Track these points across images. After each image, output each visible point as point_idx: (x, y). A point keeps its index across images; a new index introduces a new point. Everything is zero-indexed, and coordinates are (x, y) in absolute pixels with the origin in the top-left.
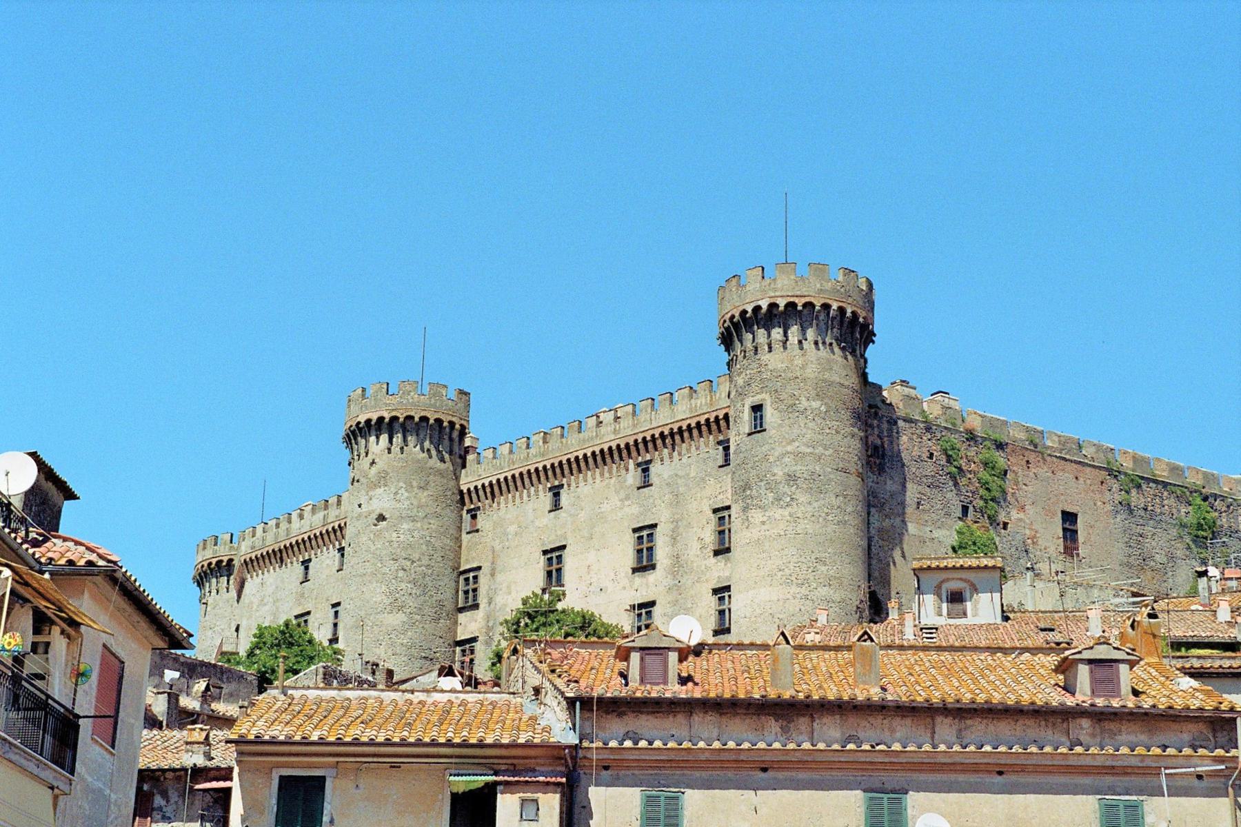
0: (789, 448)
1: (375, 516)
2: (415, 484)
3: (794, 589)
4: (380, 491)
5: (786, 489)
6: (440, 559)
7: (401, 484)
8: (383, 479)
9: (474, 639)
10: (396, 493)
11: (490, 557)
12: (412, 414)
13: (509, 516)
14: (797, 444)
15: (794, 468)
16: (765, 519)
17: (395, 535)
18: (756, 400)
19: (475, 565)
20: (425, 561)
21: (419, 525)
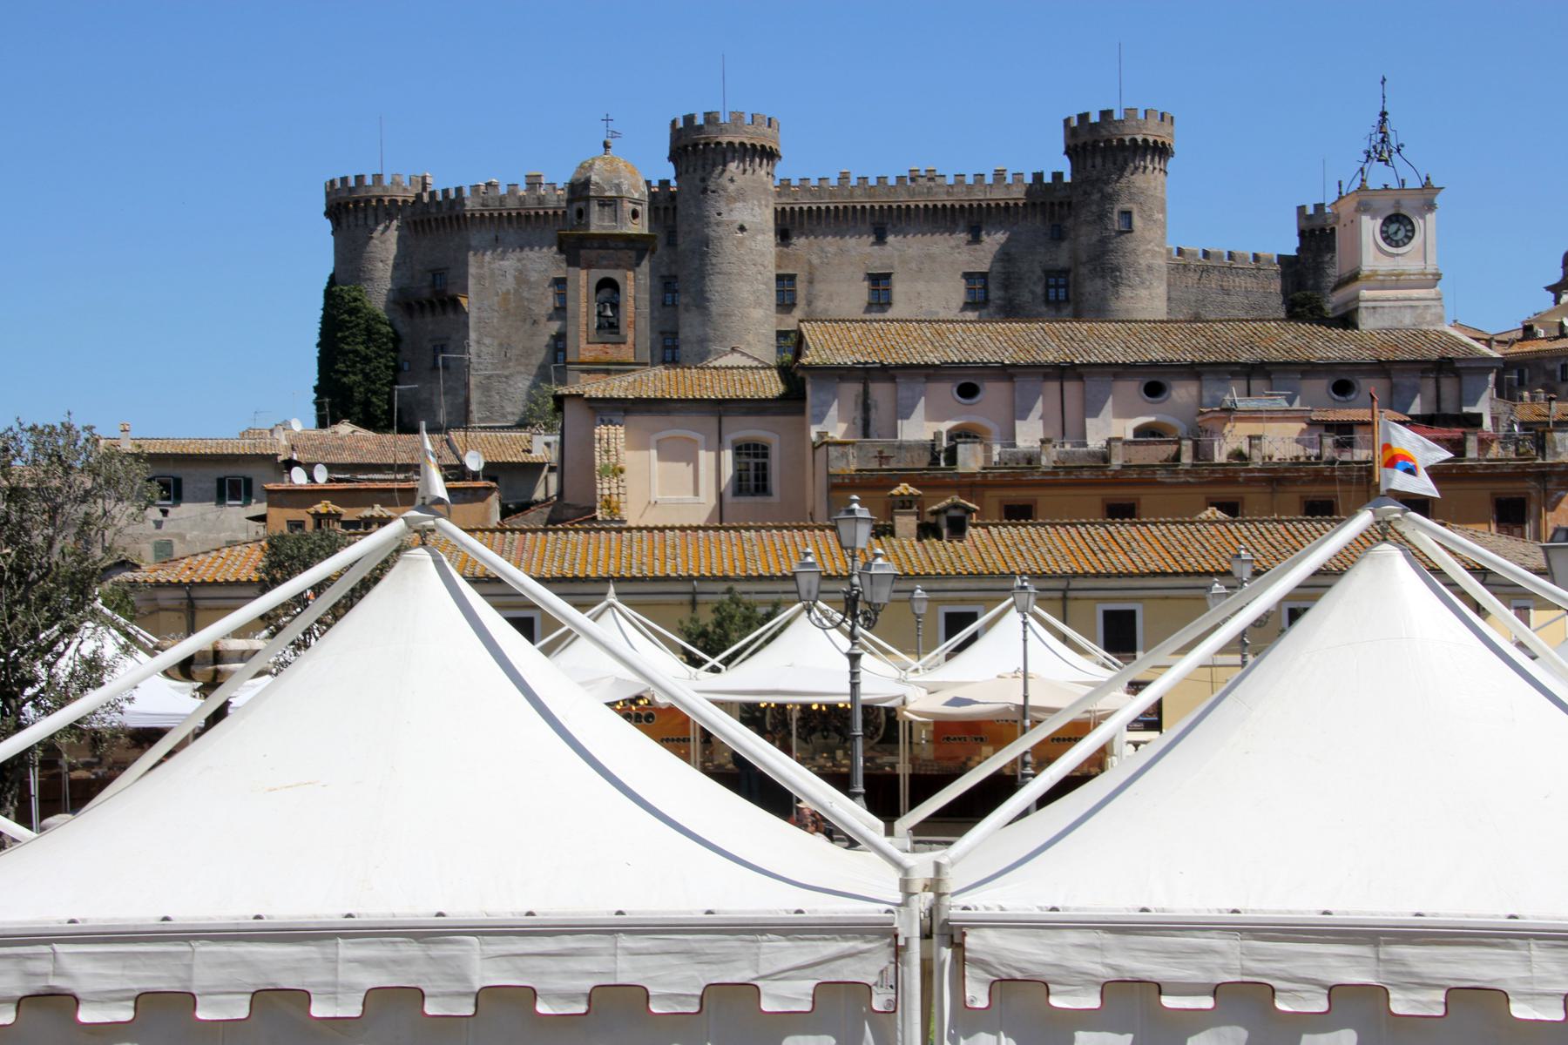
1: (736, 226)
18: (1127, 206)
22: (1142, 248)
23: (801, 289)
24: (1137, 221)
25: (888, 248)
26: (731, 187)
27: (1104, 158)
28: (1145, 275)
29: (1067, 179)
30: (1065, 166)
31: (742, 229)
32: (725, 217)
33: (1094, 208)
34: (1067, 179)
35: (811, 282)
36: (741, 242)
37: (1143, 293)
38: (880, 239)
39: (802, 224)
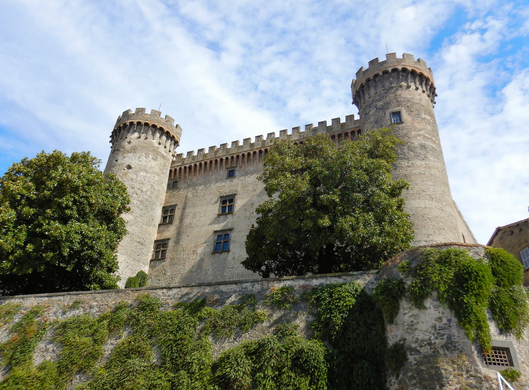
0: (420, 133)
1: (125, 165)
2: (150, 156)
3: (434, 203)
4: (129, 155)
5: (421, 151)
6: (156, 195)
7: (143, 154)
8: (134, 150)
9: (168, 239)
10: (139, 157)
11: (183, 201)
12: (156, 124)
13: (198, 182)
14: (423, 132)
15: (424, 142)
16: (410, 164)
17: (135, 176)
18: (396, 109)
19: (173, 204)
20: (149, 193)
21: (149, 175)
22: (414, 133)
23: (177, 213)
24: (405, 115)
25: (235, 181)
26: (128, 146)
27: (375, 87)
28: (418, 150)
29: (357, 117)
30: (354, 111)
31: (129, 167)
32: (120, 161)
33: (372, 119)
34: (357, 117)
35: (184, 208)
36: (126, 174)
37: (419, 163)
38: (231, 174)
39: (185, 177)
